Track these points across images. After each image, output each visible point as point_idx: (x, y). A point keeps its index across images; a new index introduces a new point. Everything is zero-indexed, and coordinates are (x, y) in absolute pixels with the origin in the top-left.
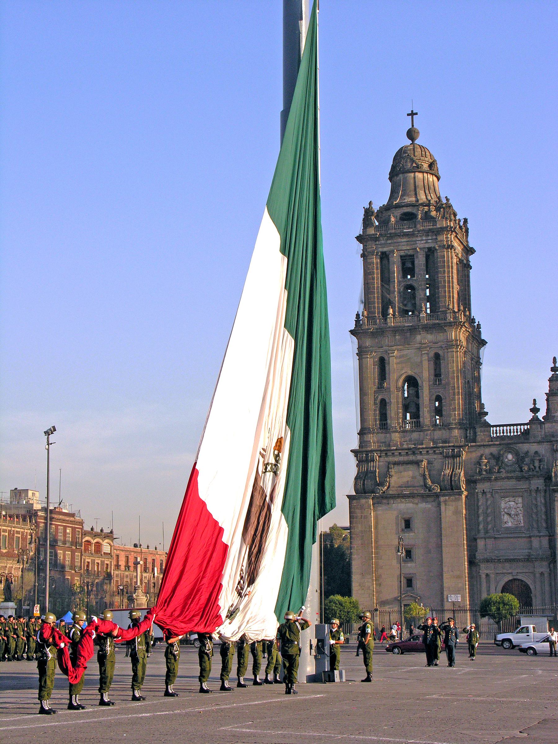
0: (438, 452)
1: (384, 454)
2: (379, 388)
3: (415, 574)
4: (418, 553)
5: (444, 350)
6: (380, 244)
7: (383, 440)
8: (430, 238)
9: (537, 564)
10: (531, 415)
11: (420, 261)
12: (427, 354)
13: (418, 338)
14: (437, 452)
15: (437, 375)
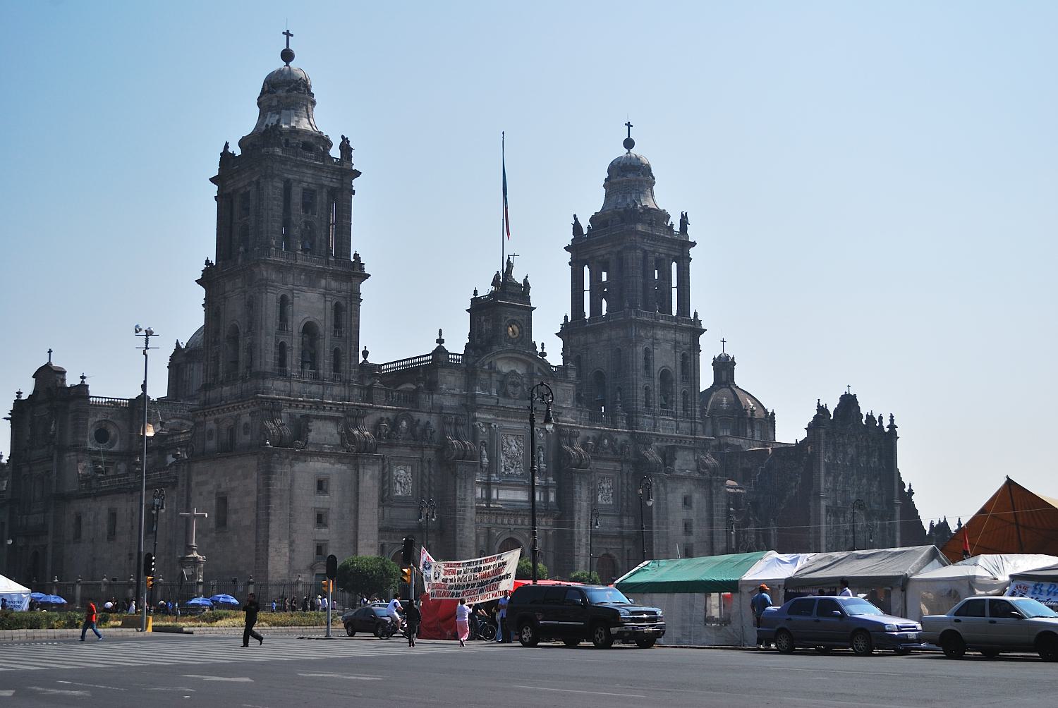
4: (332, 518)
7: (282, 389)
11: (322, 198)
13: (323, 282)
15: (337, 325)
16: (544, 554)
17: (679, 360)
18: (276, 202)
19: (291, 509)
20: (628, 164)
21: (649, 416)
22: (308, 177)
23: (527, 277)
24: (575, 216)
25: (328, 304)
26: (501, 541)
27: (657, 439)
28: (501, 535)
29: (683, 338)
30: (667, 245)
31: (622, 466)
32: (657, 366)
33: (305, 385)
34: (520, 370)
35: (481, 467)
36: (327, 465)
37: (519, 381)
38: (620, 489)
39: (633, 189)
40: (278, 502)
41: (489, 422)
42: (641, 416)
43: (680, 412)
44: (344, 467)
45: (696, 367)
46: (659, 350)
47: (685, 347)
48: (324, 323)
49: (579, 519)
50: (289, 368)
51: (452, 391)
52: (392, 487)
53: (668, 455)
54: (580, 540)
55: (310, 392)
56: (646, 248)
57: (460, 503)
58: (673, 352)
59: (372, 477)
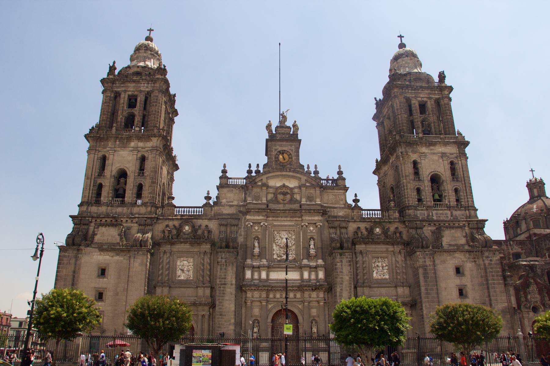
0: (135, 221)
1: (94, 221)
2: (98, 175)
3: (104, 311)
4: (108, 296)
5: (149, 153)
6: (116, 86)
7: (96, 212)
8: (150, 85)
9: (200, 308)
10: (205, 201)
11: (141, 99)
12: (137, 155)
13: (132, 144)
14: (134, 221)
15: (142, 169)
16: (318, 321)
17: (448, 166)
18: (106, 104)
20: (397, 54)
21: (423, 208)
22: (131, 88)
23: (295, 122)
24: (375, 98)
25: (135, 156)
26: (274, 311)
28: (274, 307)
29: (451, 150)
30: (428, 92)
31: (394, 247)
32: (426, 172)
33: (112, 208)
34: (292, 184)
35: (253, 256)
36: (108, 257)
37: (289, 191)
38: (394, 266)
39: (402, 66)
40: (63, 283)
41: (260, 222)
43: (453, 203)
44: (122, 259)
45: (464, 169)
46: (426, 160)
47: (453, 156)
48: (132, 168)
49: (341, 290)
50: (102, 198)
51: (231, 203)
52: (176, 273)
53: (438, 235)
55: (116, 213)
56: (408, 96)
57: (220, 281)
58: (441, 160)
59: (141, 264)
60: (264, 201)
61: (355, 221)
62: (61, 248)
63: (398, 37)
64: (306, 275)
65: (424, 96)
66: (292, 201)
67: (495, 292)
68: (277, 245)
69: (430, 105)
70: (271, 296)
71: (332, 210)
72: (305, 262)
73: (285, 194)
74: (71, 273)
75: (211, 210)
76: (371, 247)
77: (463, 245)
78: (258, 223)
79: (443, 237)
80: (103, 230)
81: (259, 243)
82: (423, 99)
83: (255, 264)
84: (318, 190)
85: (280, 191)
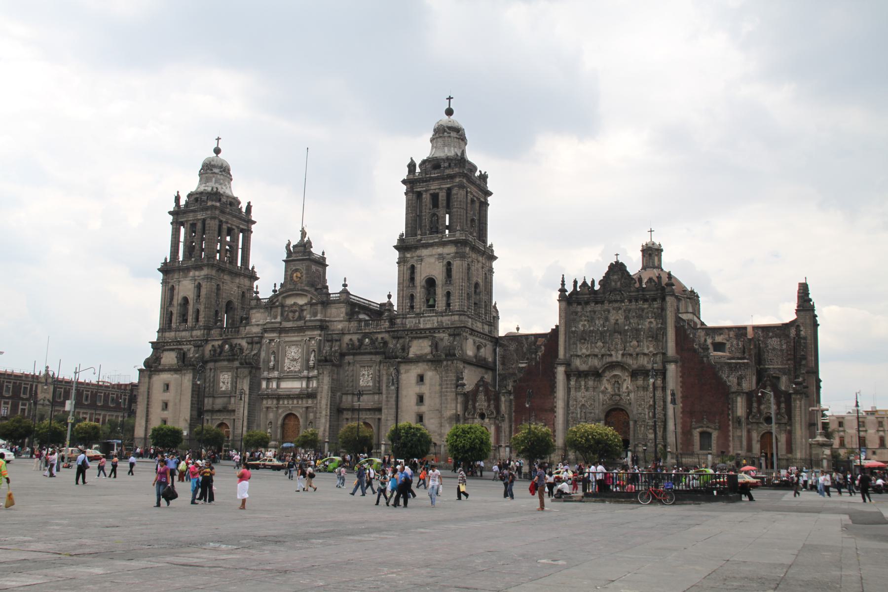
4: (170, 405)
13: (191, 274)
15: (199, 296)
19: (148, 401)
26: (283, 415)
27: (412, 333)
29: (450, 250)
34: (301, 301)
37: (297, 309)
42: (399, 318)
46: (423, 264)
48: (191, 296)
49: (321, 398)
51: (258, 323)
52: (219, 384)
54: (321, 413)
56: (419, 190)
58: (437, 262)
60: (279, 319)
61: (349, 333)
62: (141, 371)
63: (447, 99)
64: (304, 385)
65: (435, 187)
66: (300, 318)
67: (446, 399)
68: (288, 358)
69: (442, 196)
70: (281, 402)
71: (332, 323)
72: (305, 373)
73: (294, 312)
74: (146, 390)
75: (245, 329)
76: (358, 358)
77: (426, 355)
78: (271, 340)
79: (410, 347)
80: (166, 354)
81: (275, 357)
82: (434, 191)
83: (270, 375)
84: (319, 307)
85: (291, 309)
